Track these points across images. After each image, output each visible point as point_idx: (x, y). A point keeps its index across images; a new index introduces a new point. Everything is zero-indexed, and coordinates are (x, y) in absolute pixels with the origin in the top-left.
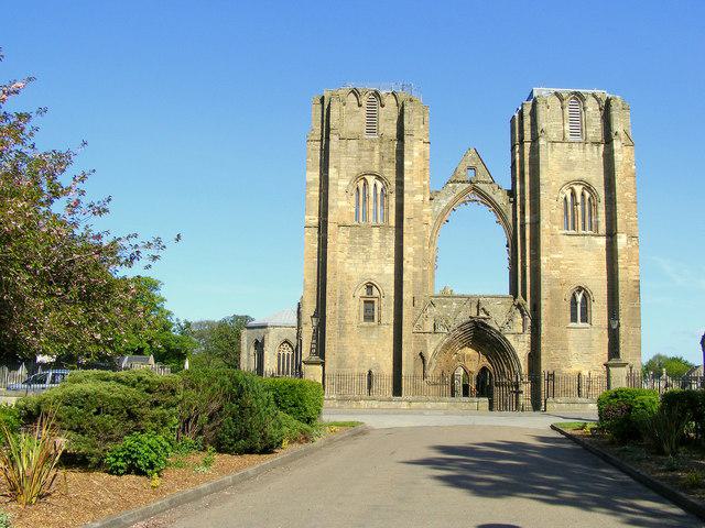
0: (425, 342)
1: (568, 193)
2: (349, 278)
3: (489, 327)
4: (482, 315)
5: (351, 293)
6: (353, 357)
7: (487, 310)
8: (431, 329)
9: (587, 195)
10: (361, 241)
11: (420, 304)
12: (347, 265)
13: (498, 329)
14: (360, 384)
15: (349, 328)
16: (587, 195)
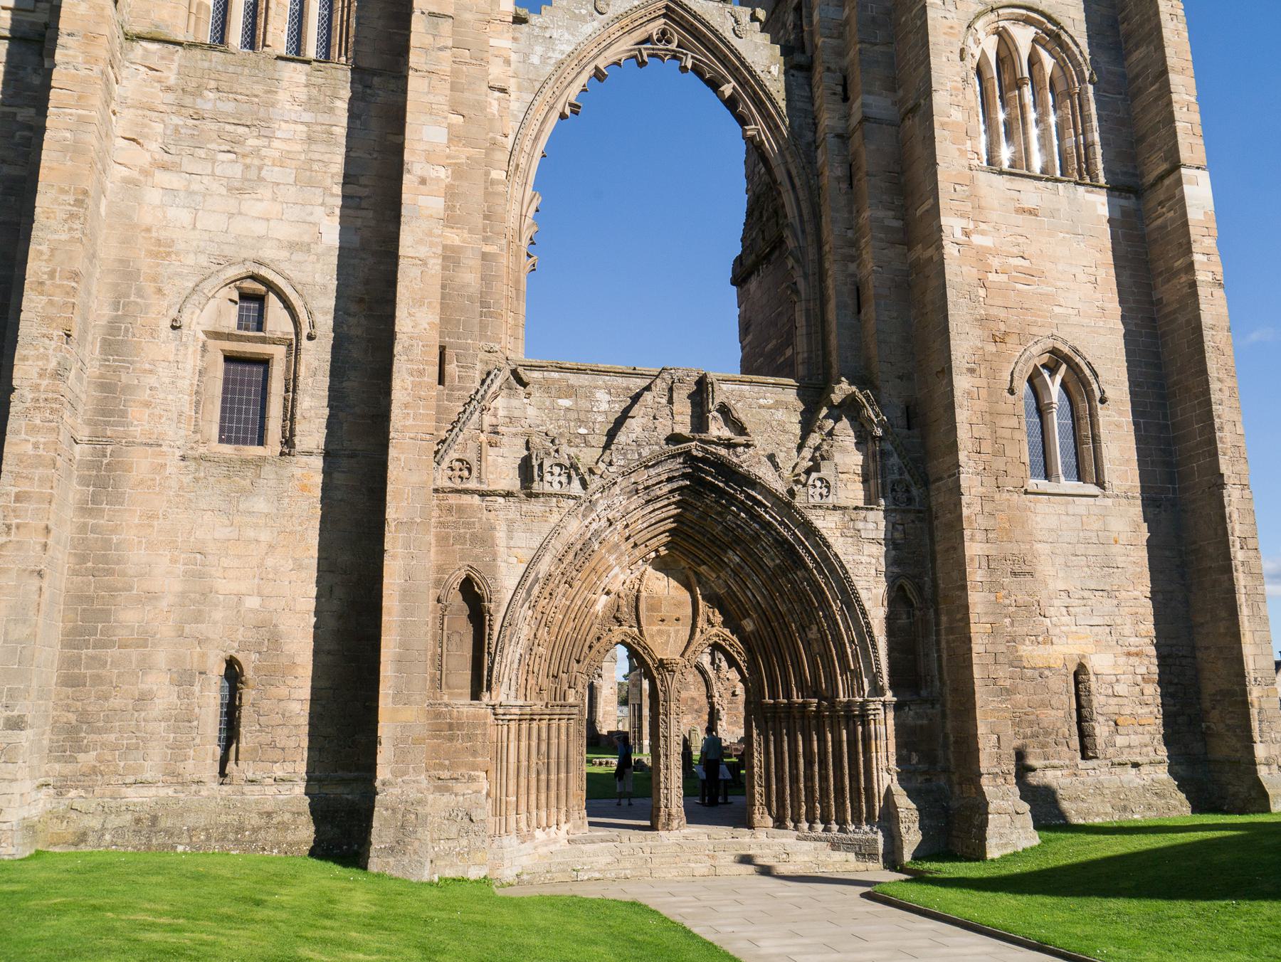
0: (484, 539)
1: (990, 46)
2: (164, 249)
3: (749, 481)
4: (717, 429)
5: (160, 311)
6: (151, 597)
7: (741, 412)
8: (511, 481)
9: (1048, 62)
10: (229, 107)
11: (466, 376)
12: (153, 196)
13: (780, 487)
14: (184, 720)
15: (140, 463)
16: (1048, 62)
